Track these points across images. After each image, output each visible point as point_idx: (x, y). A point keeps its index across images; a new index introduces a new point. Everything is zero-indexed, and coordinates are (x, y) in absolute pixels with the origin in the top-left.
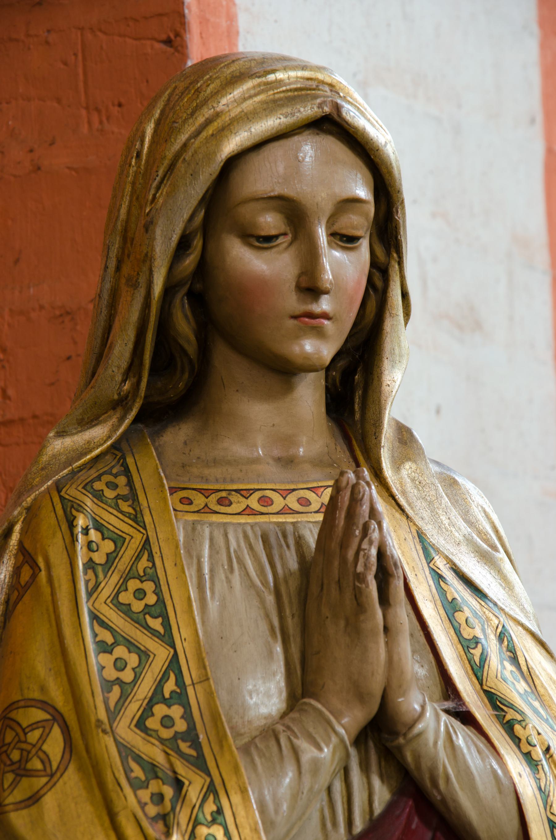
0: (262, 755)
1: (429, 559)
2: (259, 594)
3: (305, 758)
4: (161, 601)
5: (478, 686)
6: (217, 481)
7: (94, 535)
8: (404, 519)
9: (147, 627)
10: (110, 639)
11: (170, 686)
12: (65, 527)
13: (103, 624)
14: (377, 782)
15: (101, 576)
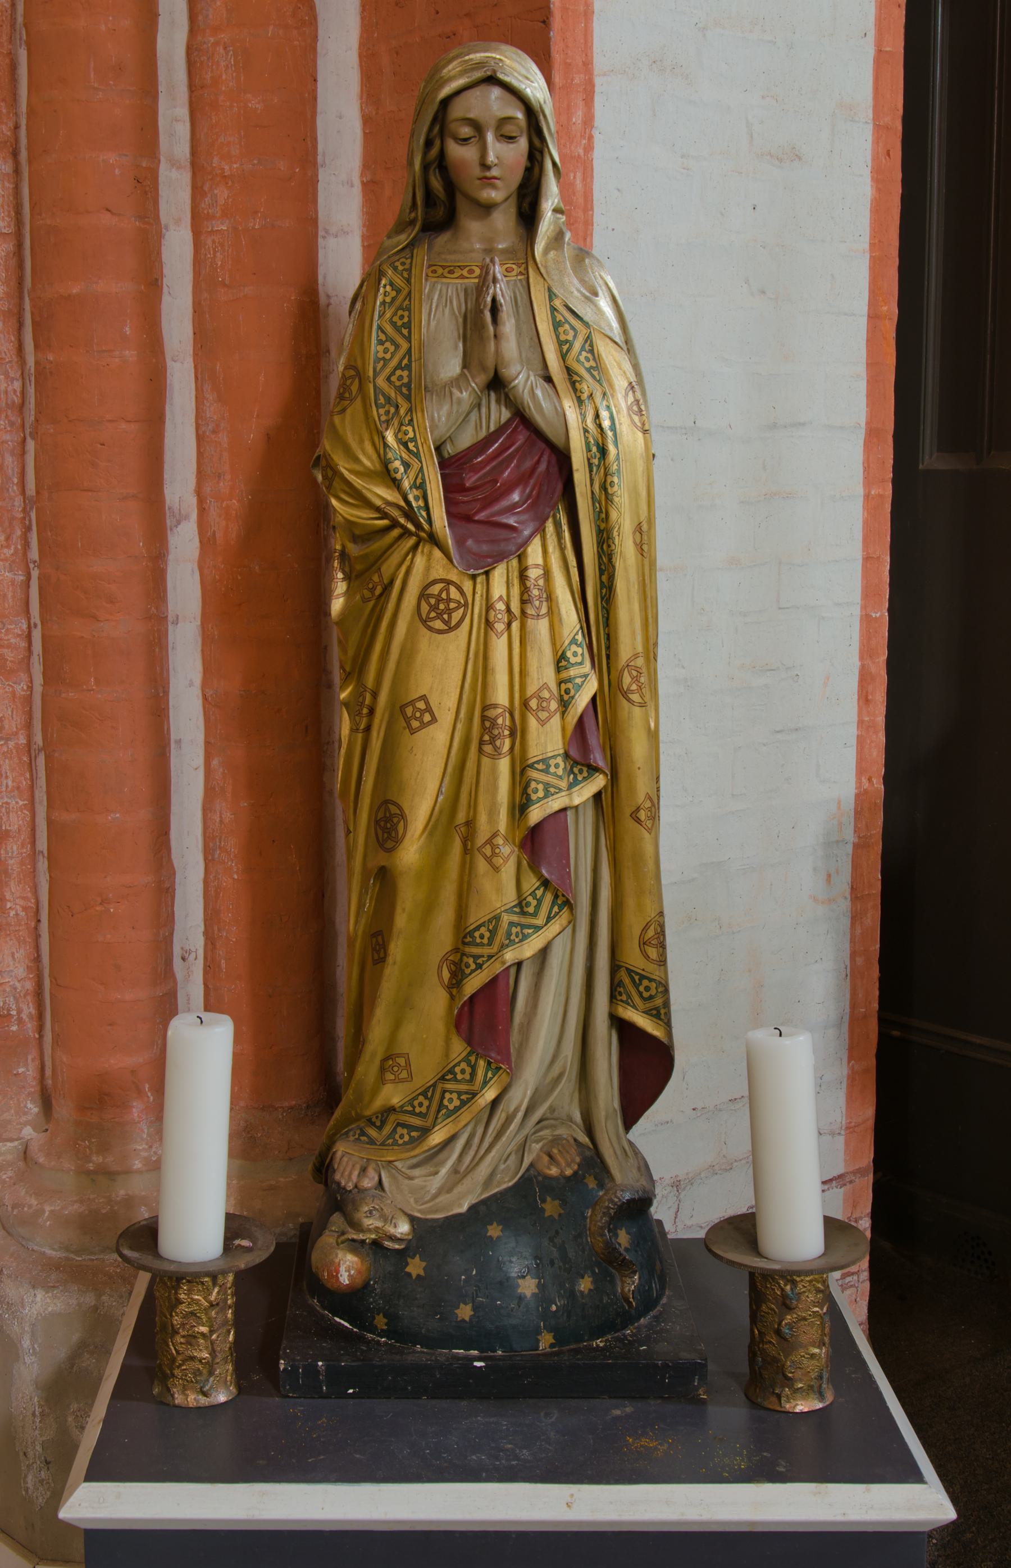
0: (437, 395)
1: (551, 300)
2: (456, 317)
3: (454, 398)
4: (410, 322)
5: (562, 364)
6: (451, 262)
7: (388, 288)
8: (542, 280)
9: (401, 333)
10: (384, 339)
11: (405, 361)
12: (377, 282)
13: (383, 332)
14: (503, 409)
15: (387, 308)
